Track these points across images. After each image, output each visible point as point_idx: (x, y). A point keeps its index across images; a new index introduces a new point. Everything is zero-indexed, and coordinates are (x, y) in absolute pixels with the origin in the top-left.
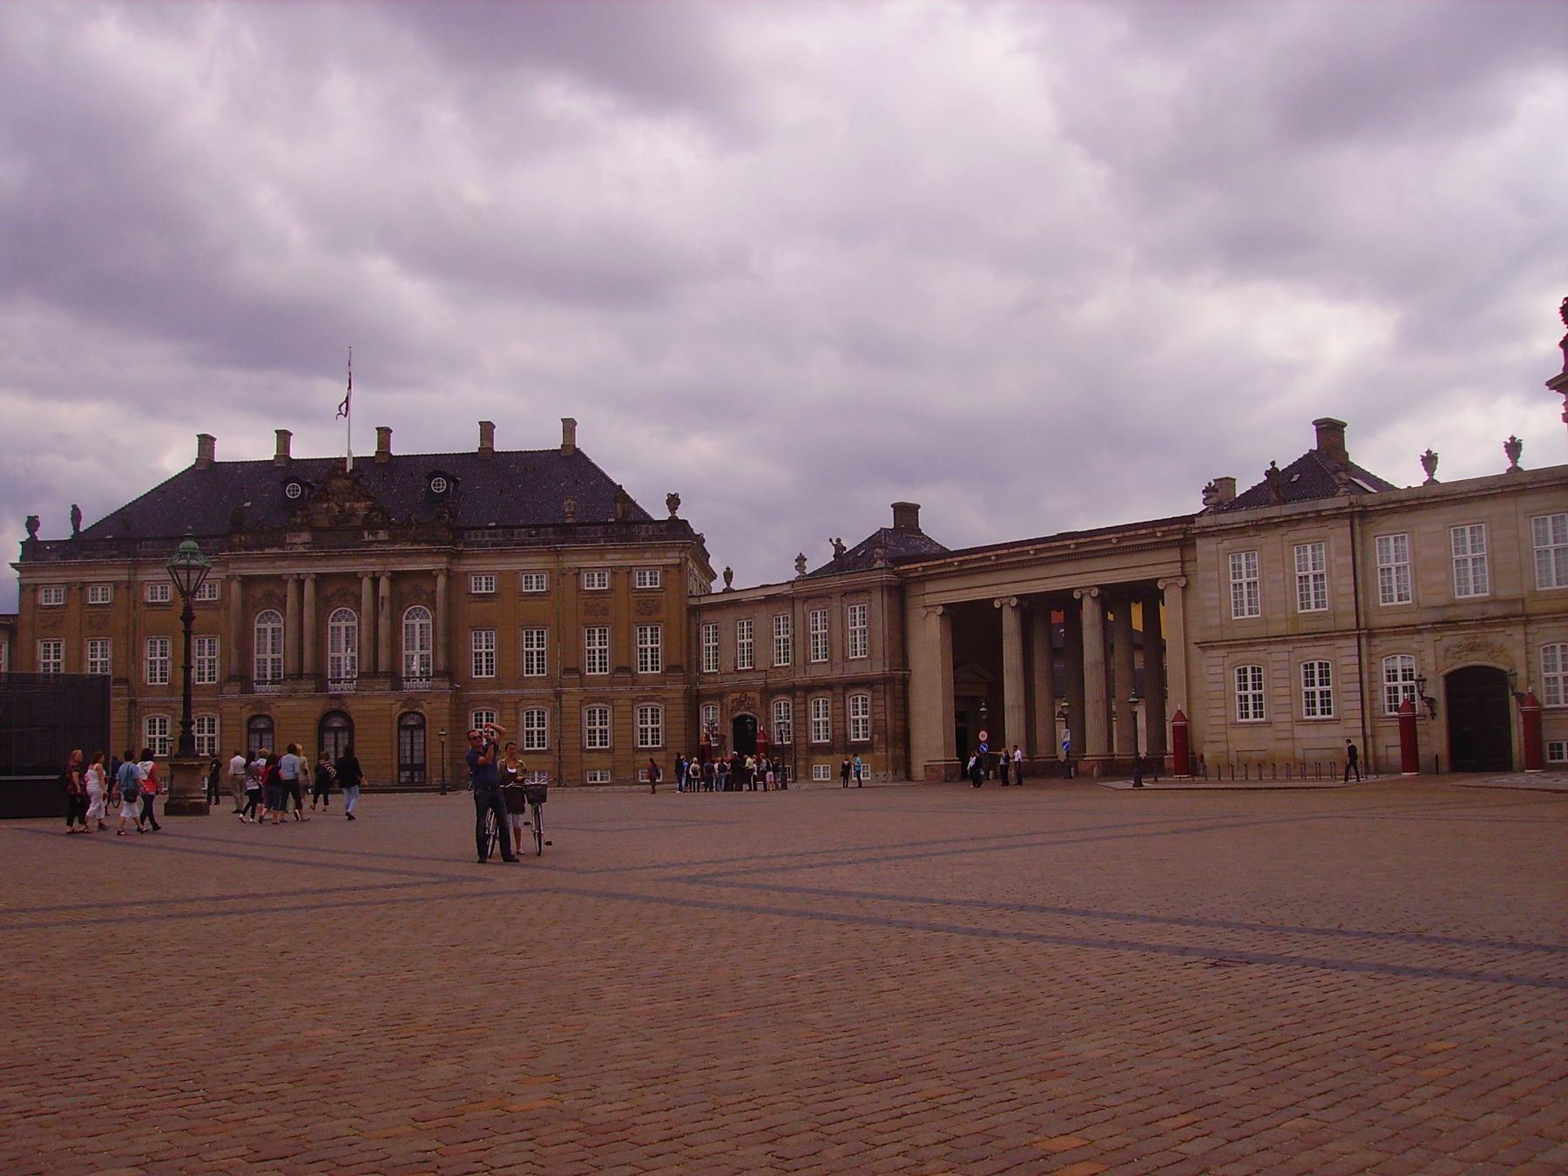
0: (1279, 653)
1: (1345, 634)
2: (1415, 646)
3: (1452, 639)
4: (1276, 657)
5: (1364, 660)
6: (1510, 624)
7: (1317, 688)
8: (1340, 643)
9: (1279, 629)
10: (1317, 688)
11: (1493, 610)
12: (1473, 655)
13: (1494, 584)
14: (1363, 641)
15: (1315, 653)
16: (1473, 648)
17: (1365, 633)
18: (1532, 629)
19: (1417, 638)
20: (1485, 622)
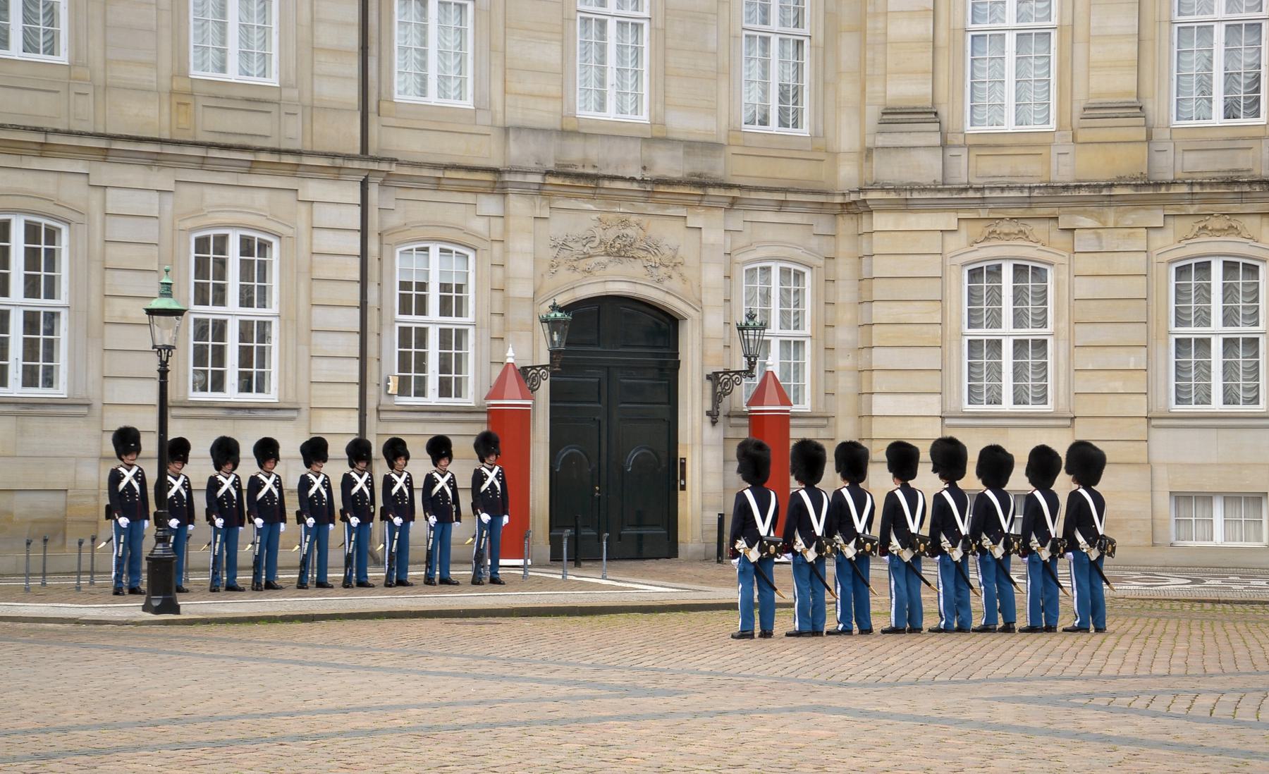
0: (134, 193)
1: (334, 165)
2: (479, 225)
3: (579, 218)
4: (118, 201)
5: (373, 247)
6: (700, 203)
7: (232, 311)
8: (313, 189)
9: (143, 116)
10: (232, 311)
11: (667, 164)
12: (615, 268)
13: (661, 98)
14: (373, 191)
15: (234, 206)
16: (621, 251)
17: (368, 167)
18: (737, 220)
19: (490, 205)
20: (656, 188)
